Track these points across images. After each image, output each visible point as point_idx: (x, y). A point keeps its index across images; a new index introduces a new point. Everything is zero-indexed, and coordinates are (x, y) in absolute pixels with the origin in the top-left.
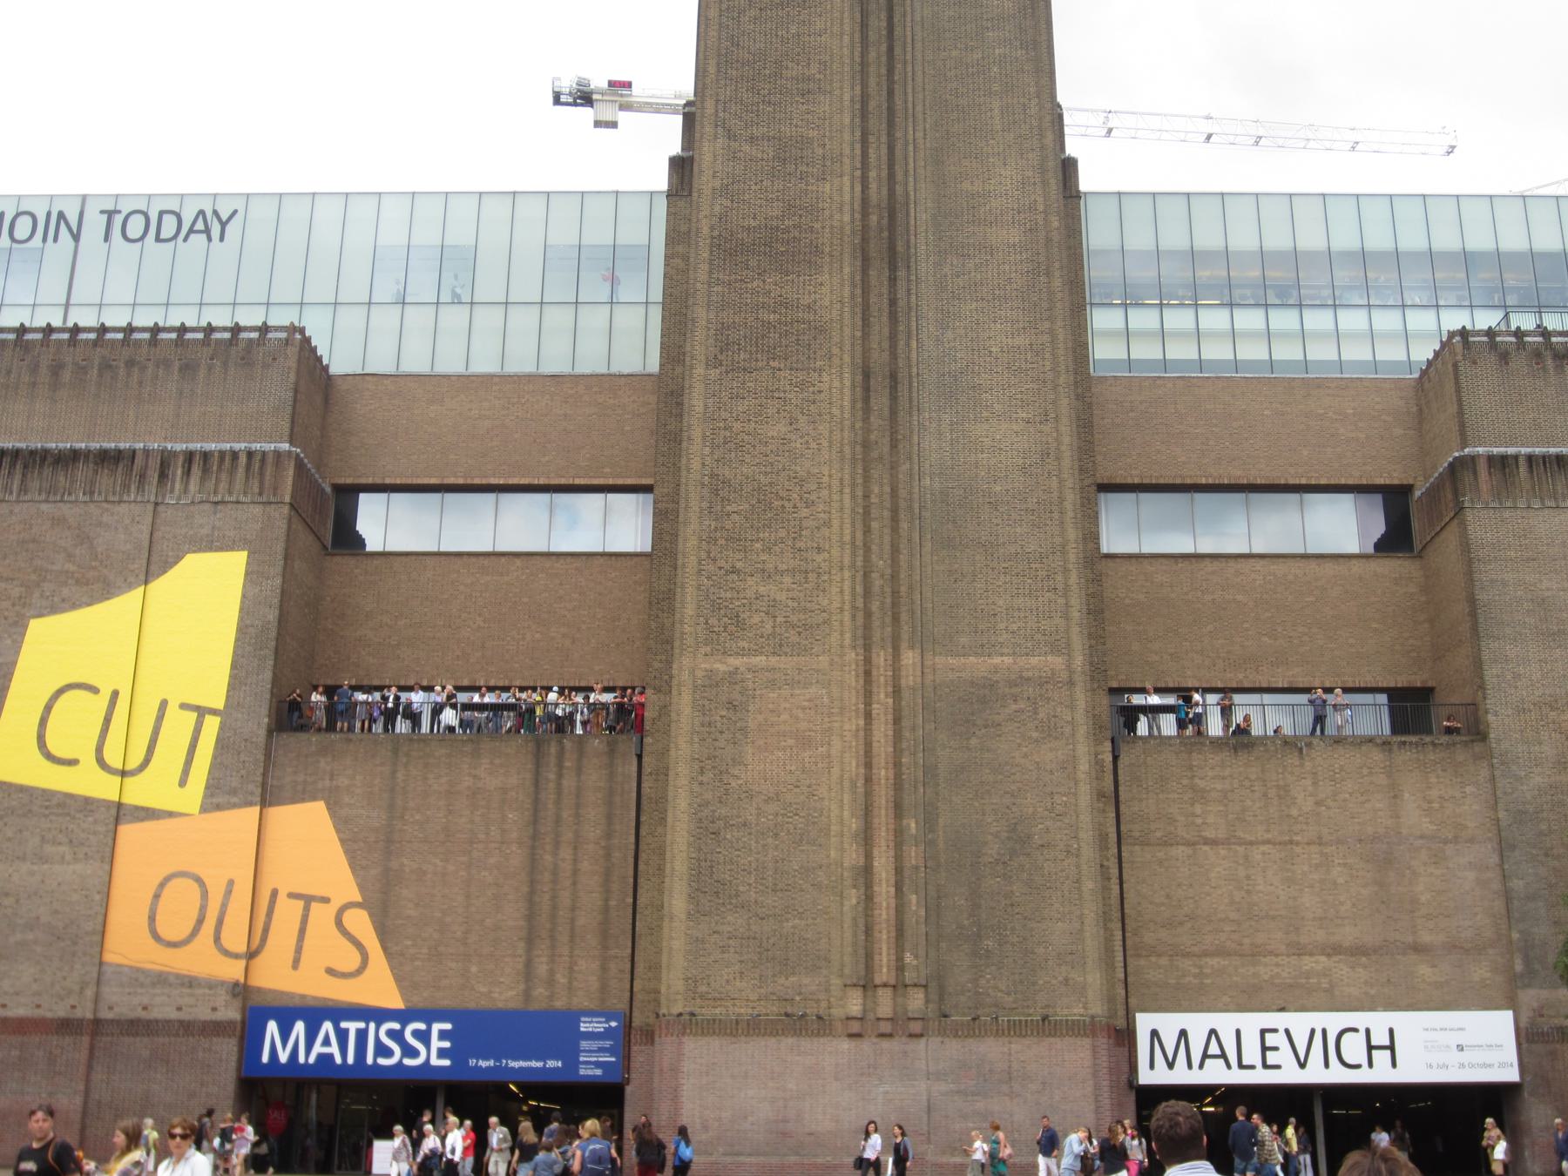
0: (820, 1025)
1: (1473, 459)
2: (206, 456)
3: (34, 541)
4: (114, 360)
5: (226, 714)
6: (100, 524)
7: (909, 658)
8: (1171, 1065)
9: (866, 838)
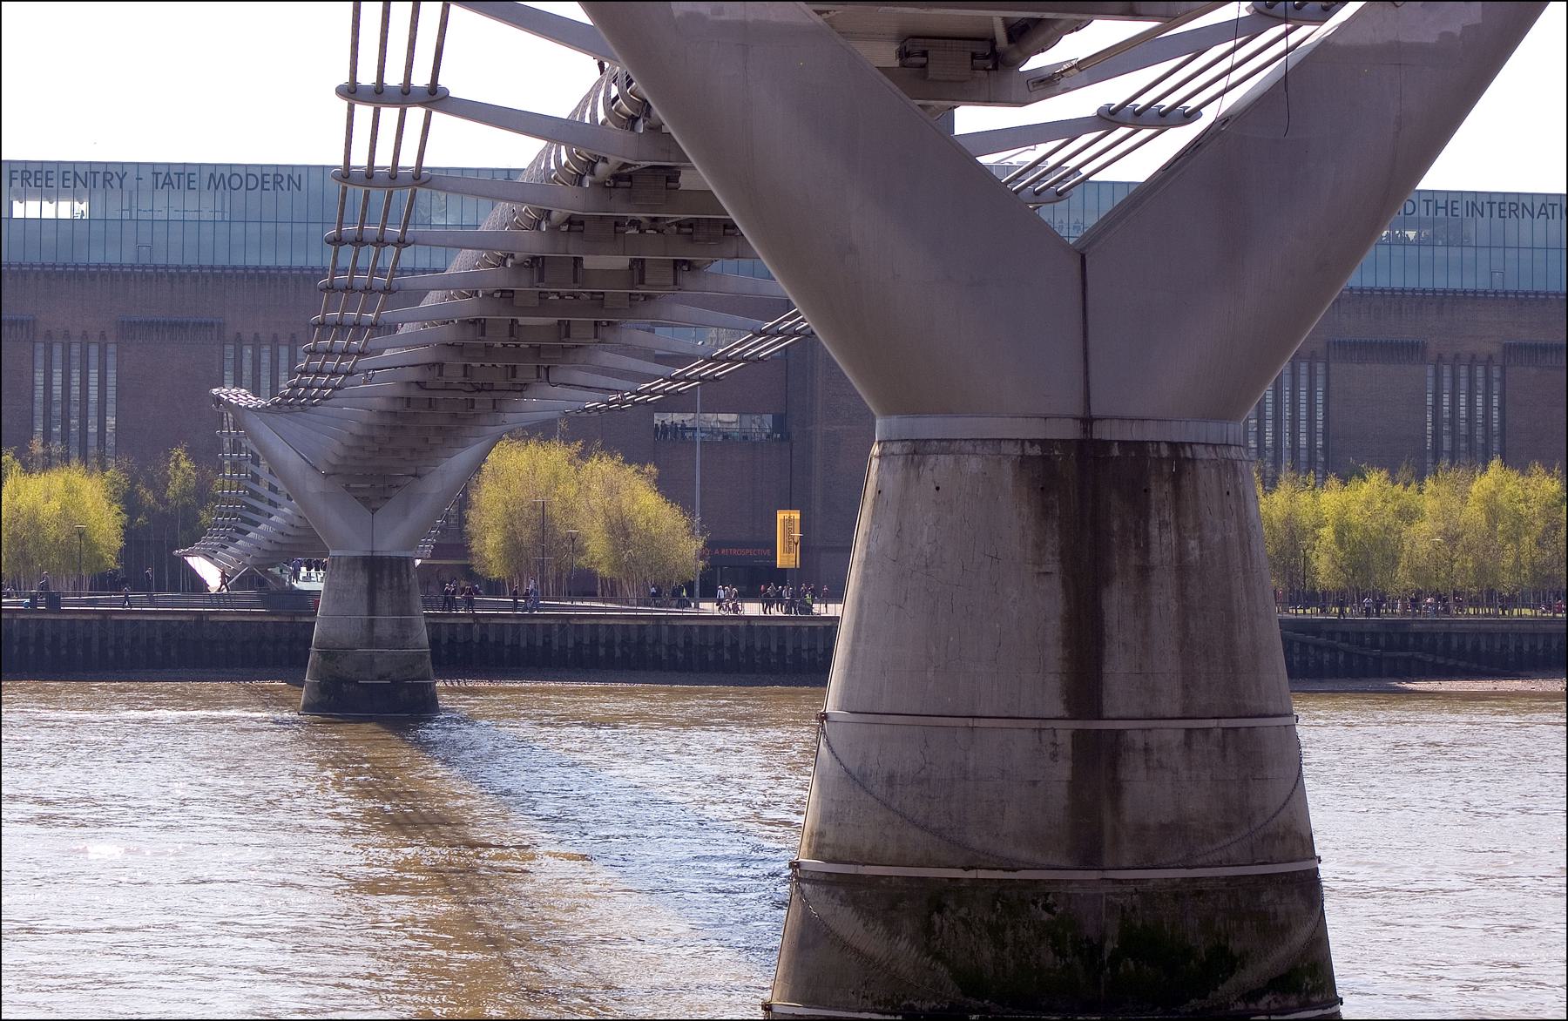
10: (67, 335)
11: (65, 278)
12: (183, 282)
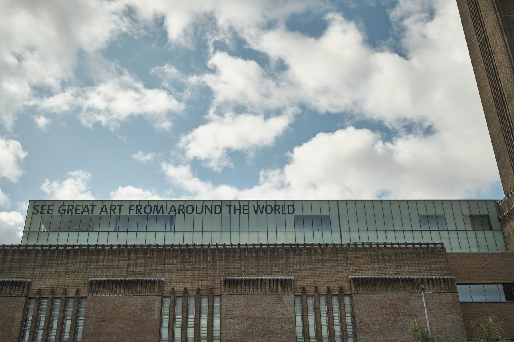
2: (432, 279)
3: (394, 304)
4: (398, 253)
6: (410, 299)
10: (52, 292)
11: (56, 253)
12: (137, 254)
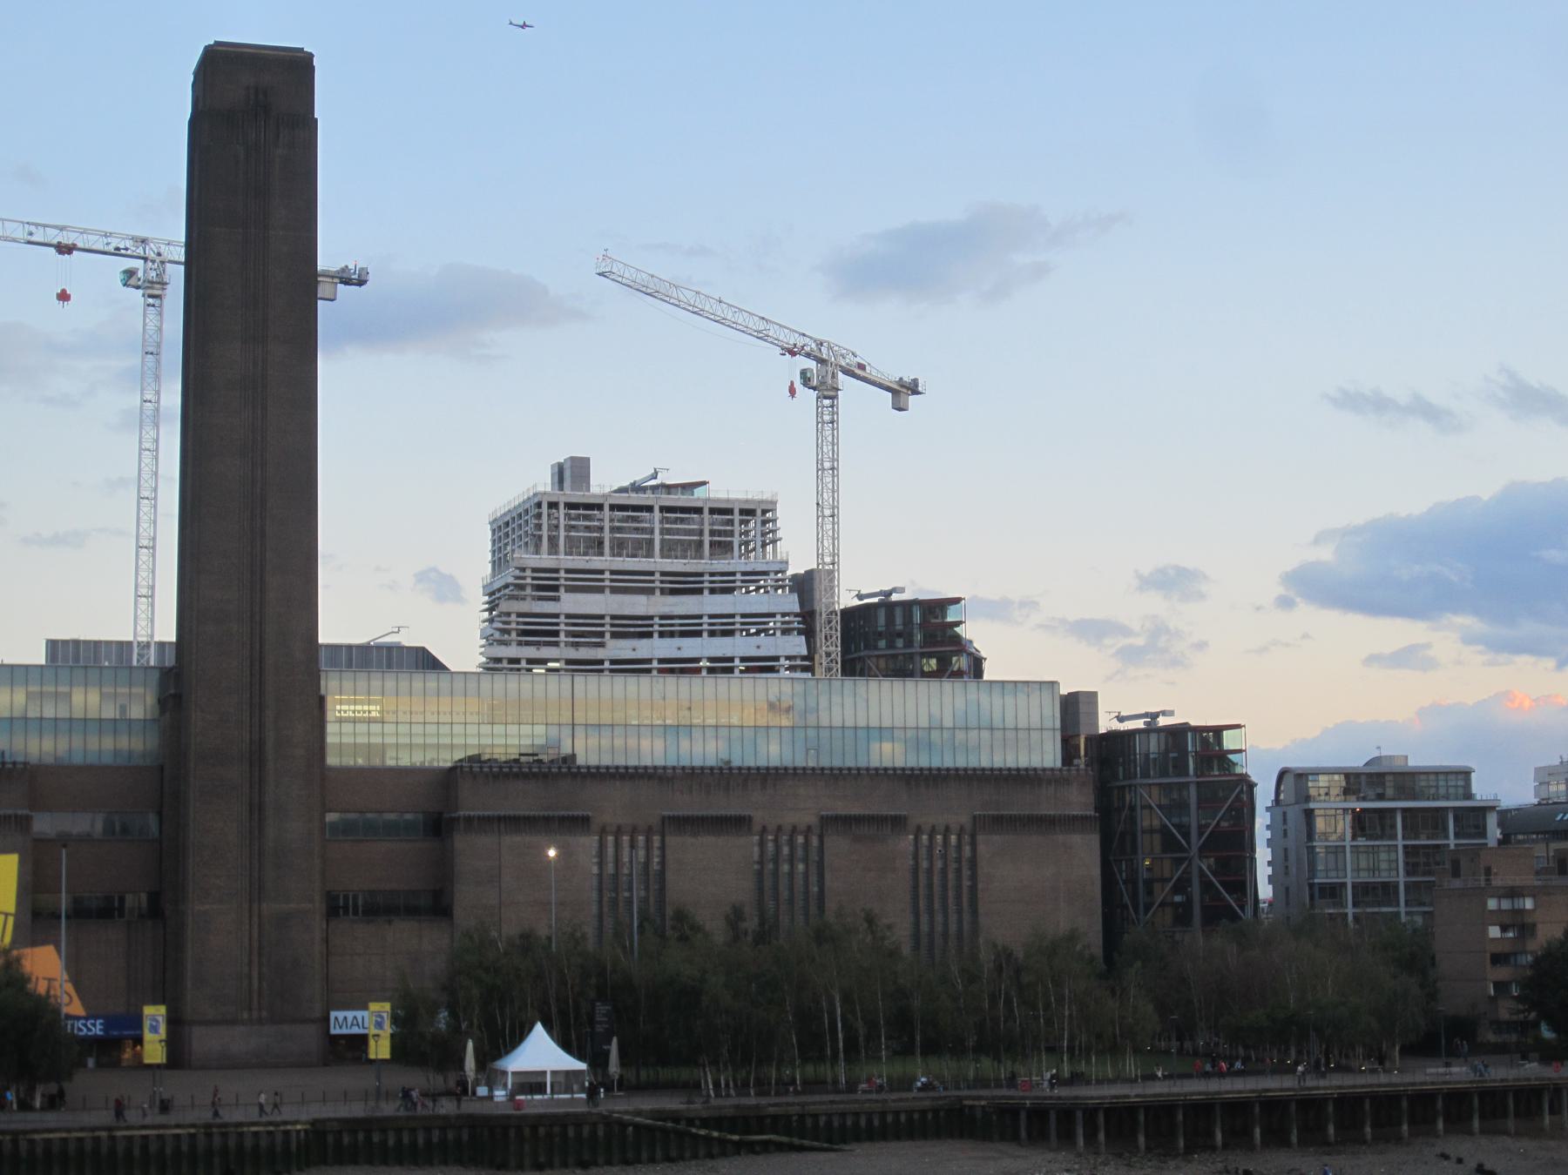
0: (233, 1022)
1: (459, 818)
5: (17, 916)
7: (264, 906)
8: (341, 1027)
9: (250, 963)
